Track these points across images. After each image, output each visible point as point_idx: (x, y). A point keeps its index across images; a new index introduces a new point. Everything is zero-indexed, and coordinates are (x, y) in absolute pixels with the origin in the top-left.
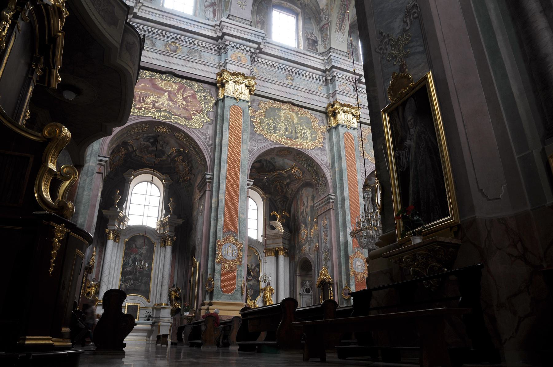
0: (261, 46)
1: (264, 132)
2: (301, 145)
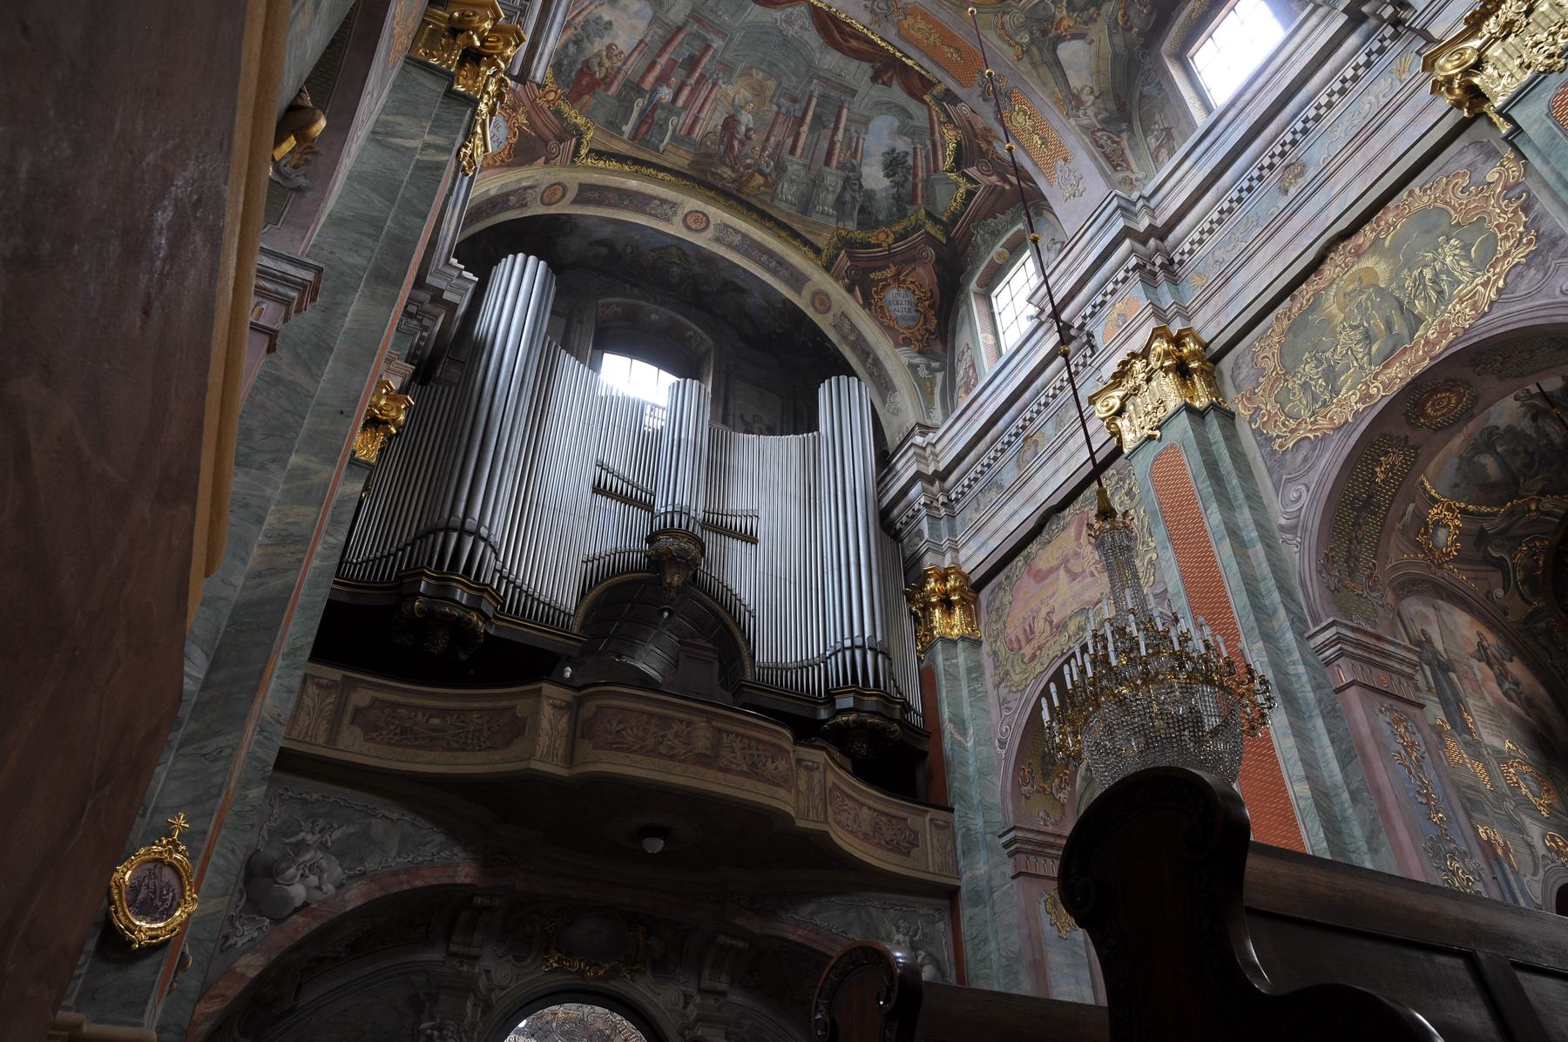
0: (1143, 224)
1: (1304, 426)
2: (1443, 333)
